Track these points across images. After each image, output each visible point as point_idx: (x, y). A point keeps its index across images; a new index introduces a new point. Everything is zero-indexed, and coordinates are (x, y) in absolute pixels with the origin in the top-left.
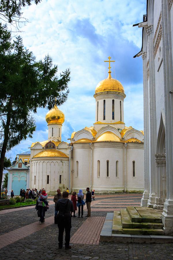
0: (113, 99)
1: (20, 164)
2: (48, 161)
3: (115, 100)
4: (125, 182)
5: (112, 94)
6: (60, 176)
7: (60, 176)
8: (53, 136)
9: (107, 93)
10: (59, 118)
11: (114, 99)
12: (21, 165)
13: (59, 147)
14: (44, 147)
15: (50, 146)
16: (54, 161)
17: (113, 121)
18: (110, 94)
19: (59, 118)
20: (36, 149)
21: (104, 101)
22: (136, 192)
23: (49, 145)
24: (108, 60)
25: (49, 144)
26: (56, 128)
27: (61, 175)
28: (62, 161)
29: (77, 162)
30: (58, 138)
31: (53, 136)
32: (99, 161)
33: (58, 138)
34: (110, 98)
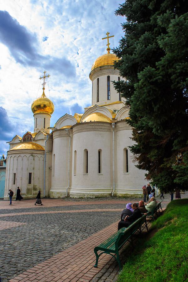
0: (108, 75)
1: (2, 162)
2: (15, 155)
3: (111, 76)
4: (114, 181)
5: (107, 69)
6: (30, 174)
7: (30, 174)
8: (36, 128)
9: (101, 70)
10: (45, 106)
11: (109, 75)
12: (3, 163)
13: (36, 139)
14: (22, 140)
15: (28, 139)
16: (22, 155)
17: (108, 102)
18: (105, 69)
19: (45, 106)
20: (15, 143)
21: (98, 79)
22: (128, 196)
23: (26, 137)
24: (107, 36)
25: (27, 136)
26: (41, 119)
27: (30, 172)
28: (34, 155)
29: (54, 154)
30: (43, 129)
31: (36, 128)
32: (75, 151)
33: (43, 129)
34: (104, 74)
